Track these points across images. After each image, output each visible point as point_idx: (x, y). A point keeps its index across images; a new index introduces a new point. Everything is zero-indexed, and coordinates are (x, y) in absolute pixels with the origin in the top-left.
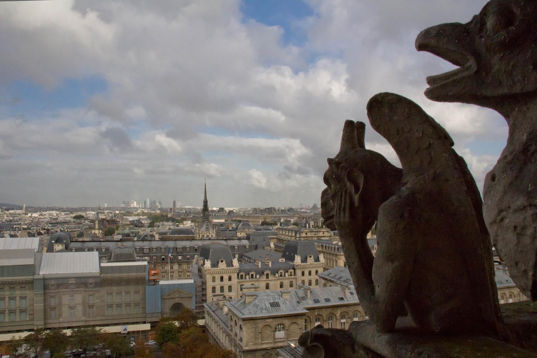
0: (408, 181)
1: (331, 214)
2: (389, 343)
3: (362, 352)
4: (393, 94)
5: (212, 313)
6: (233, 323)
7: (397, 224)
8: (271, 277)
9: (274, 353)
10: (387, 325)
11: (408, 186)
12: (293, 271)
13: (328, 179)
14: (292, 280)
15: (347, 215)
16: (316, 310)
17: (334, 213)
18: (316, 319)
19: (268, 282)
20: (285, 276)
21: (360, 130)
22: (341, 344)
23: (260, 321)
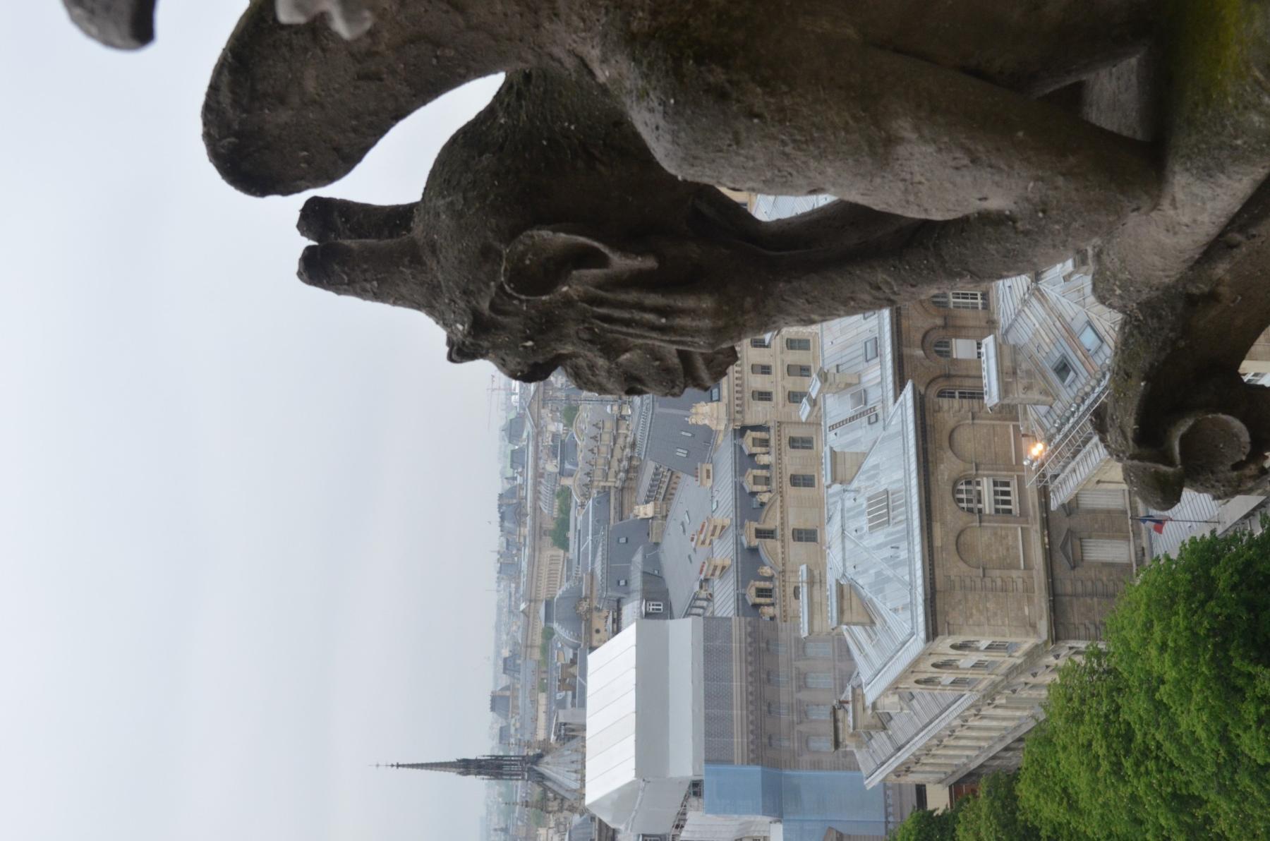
0: (572, 53)
1: (675, 361)
2: (1207, 173)
3: (1221, 269)
4: (214, 88)
5: (904, 755)
6: (947, 677)
7: (752, 114)
8: (772, 522)
9: (1065, 524)
10: (1137, 164)
11: (593, 53)
12: (750, 435)
13: (536, 366)
14: (785, 441)
15: (689, 302)
16: (906, 351)
17: (670, 350)
18: (940, 353)
19: (789, 533)
20: (766, 467)
21: (339, 222)
22: (1182, 343)
23: (937, 572)
